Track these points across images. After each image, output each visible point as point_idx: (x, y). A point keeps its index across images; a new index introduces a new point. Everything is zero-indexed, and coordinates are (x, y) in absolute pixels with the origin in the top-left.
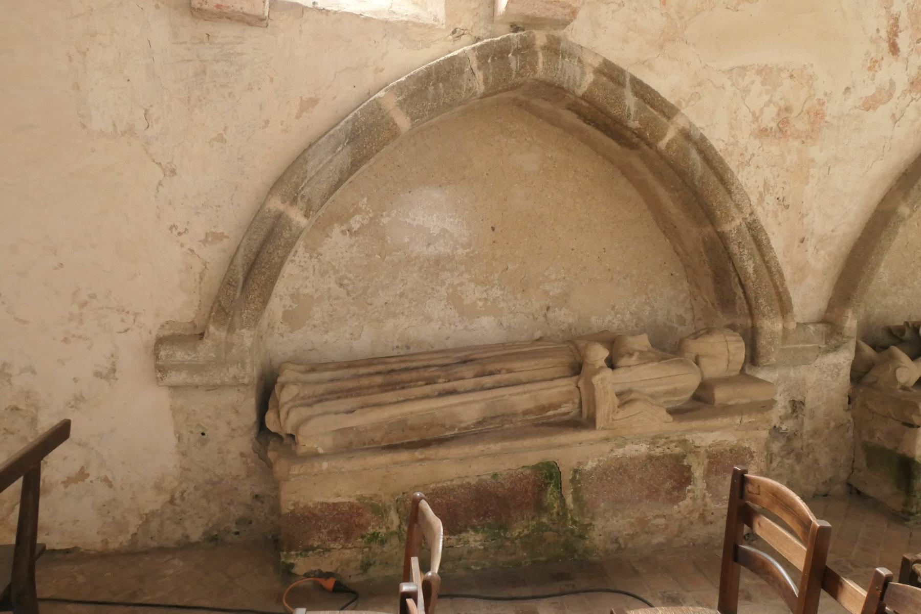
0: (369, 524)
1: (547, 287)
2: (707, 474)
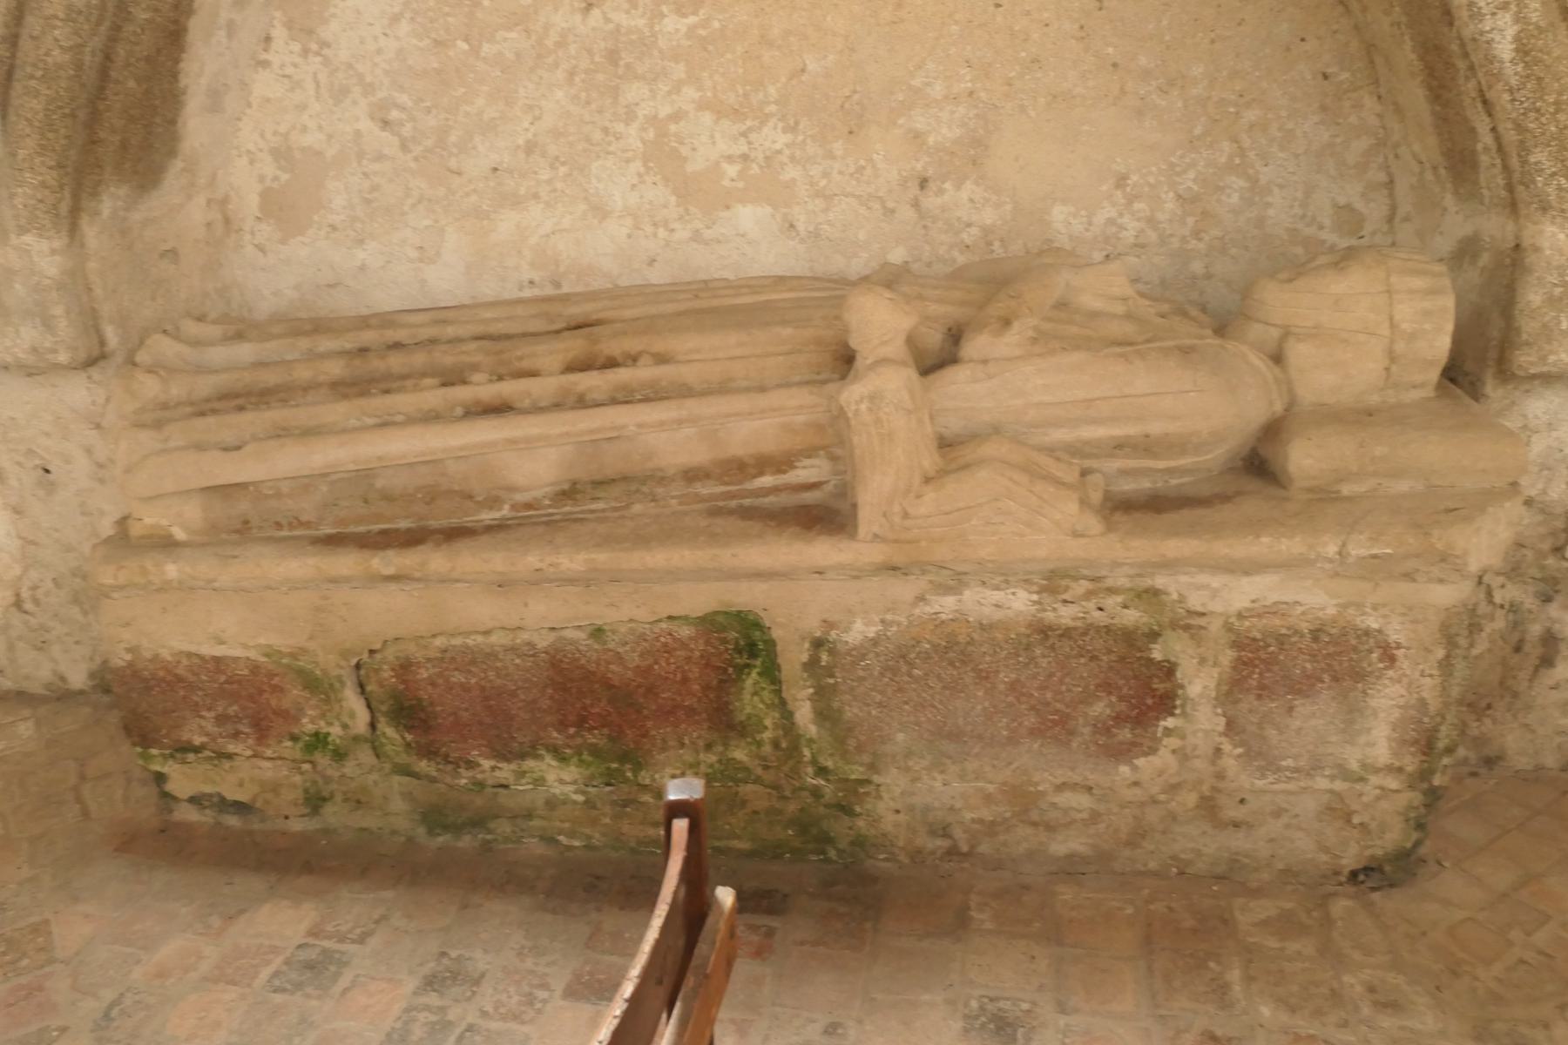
0: (301, 710)
1: (920, 122)
2: (1232, 690)
